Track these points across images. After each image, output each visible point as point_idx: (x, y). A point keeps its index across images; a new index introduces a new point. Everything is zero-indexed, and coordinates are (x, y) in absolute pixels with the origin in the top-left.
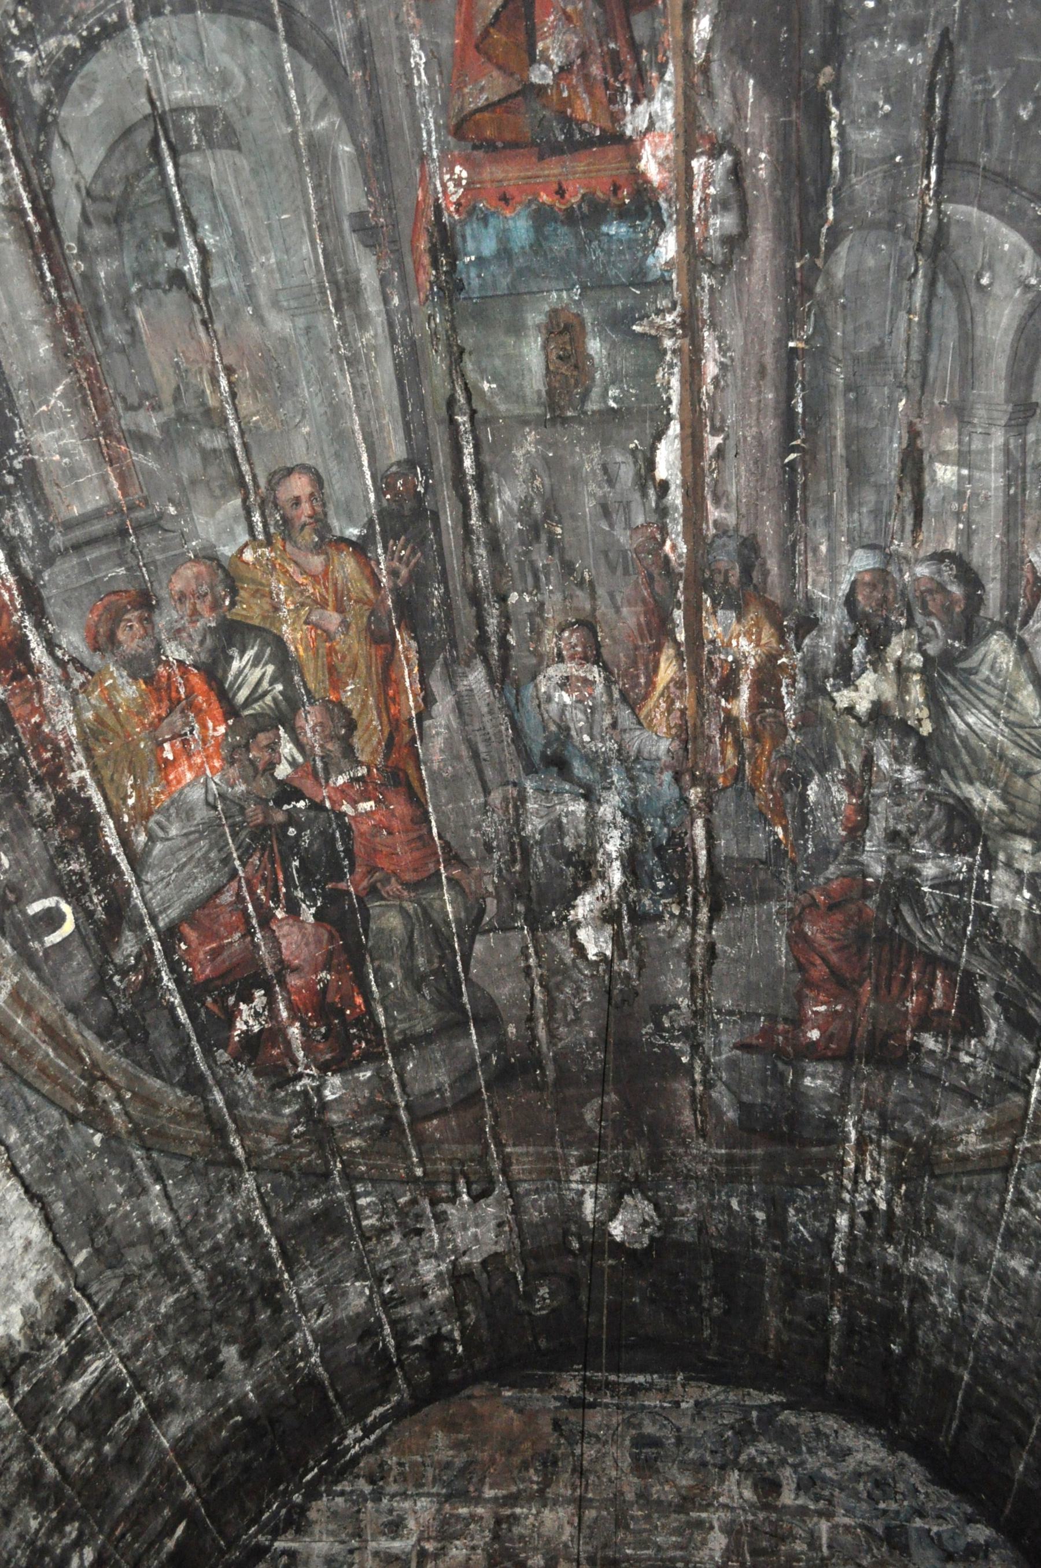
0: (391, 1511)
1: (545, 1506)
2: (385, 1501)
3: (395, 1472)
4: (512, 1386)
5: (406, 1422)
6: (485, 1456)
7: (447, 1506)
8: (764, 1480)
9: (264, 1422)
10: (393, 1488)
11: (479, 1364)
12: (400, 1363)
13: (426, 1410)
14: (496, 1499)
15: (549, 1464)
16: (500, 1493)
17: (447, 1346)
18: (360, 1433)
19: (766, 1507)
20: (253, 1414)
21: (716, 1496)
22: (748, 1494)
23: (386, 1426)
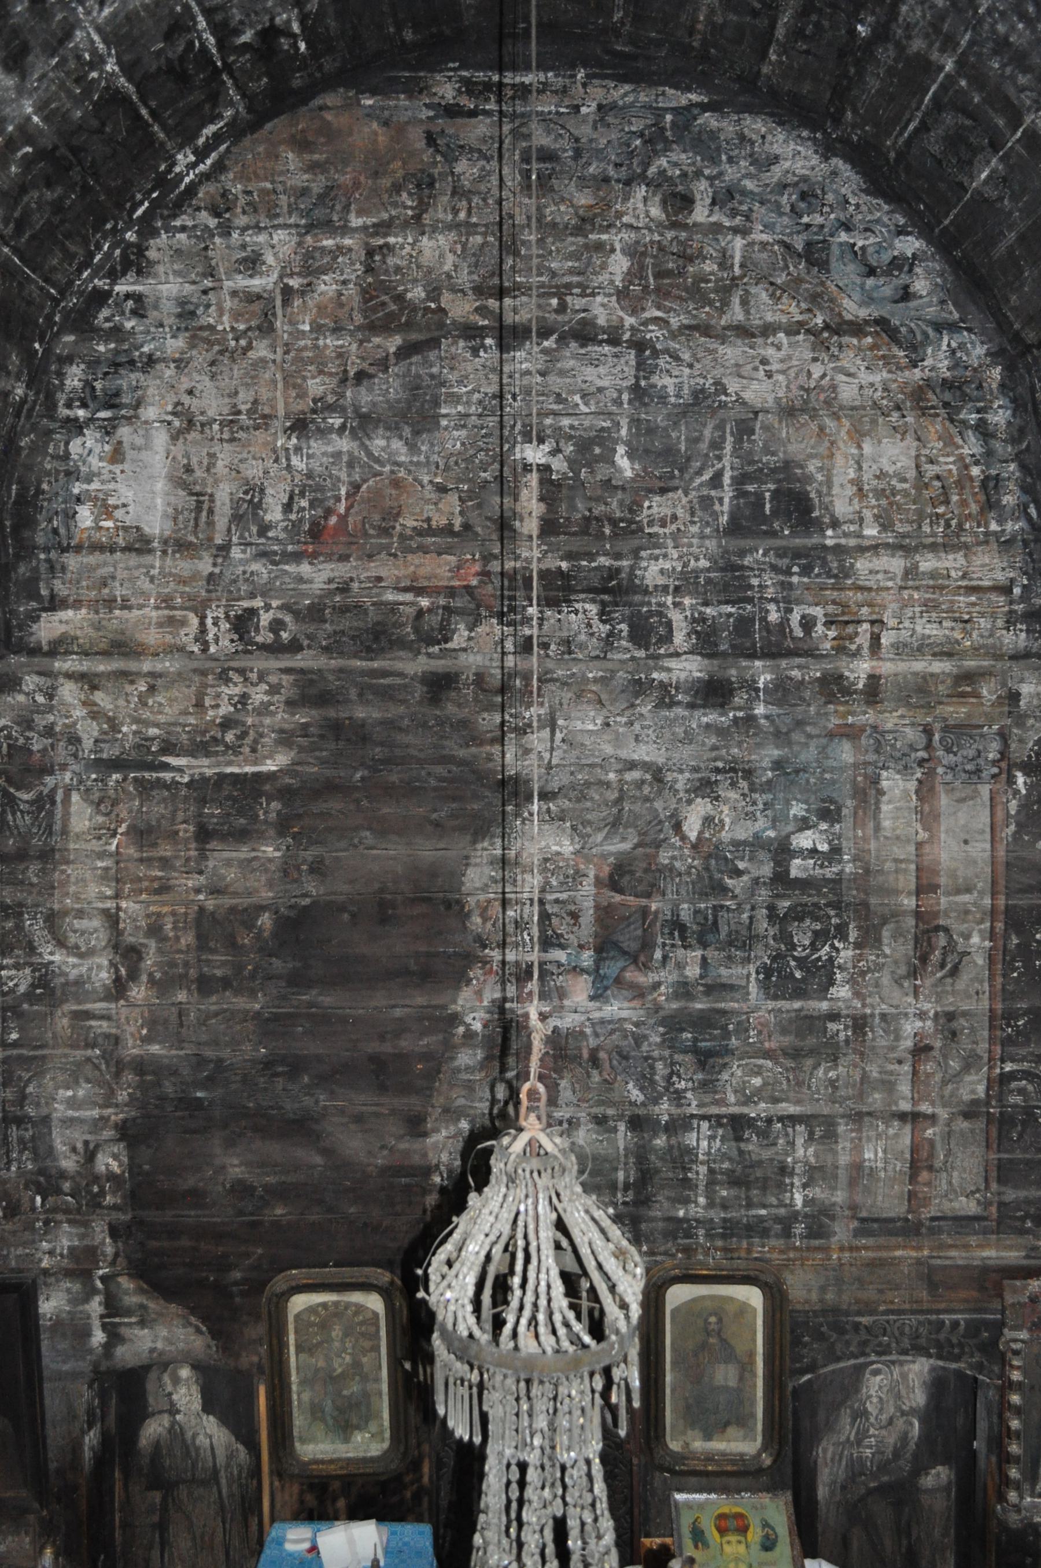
0: (244, 246)
1: (423, 233)
2: (235, 235)
3: (242, 201)
4: (373, 93)
5: (247, 141)
6: (346, 179)
7: (309, 239)
8: (674, 195)
9: (63, 150)
10: (242, 220)
11: (329, 64)
12: (228, 67)
13: (268, 126)
14: (365, 228)
15: (425, 185)
16: (370, 221)
17: (284, 43)
18: (192, 158)
19: (674, 225)
20: (47, 143)
21: (619, 215)
22: (656, 212)
23: (223, 148)
